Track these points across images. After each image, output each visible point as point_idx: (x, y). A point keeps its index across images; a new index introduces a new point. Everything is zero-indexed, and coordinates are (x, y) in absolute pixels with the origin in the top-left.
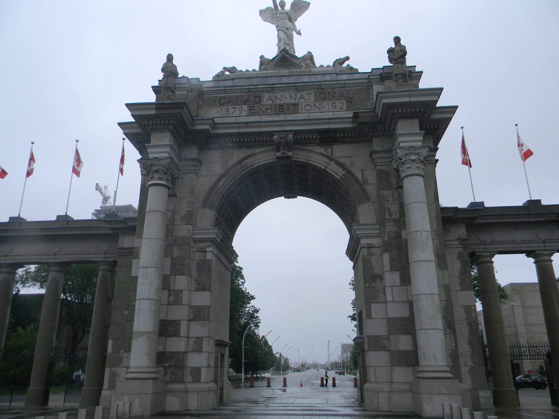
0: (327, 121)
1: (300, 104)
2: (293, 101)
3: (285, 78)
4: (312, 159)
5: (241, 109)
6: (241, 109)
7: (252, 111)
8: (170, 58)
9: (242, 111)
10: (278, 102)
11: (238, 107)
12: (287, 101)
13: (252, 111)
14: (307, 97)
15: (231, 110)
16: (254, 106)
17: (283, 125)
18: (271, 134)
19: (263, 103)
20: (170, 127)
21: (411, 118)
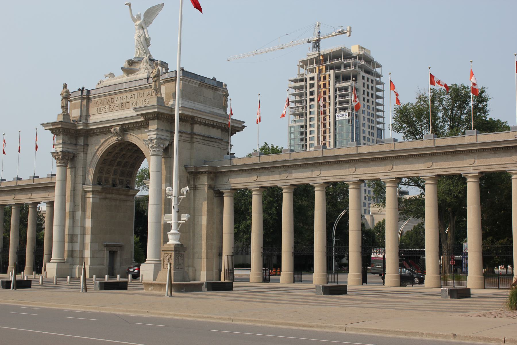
0: (132, 118)
1: (130, 102)
2: (128, 100)
3: (125, 84)
4: (132, 140)
5: (105, 108)
6: (105, 108)
7: (110, 109)
8: (65, 86)
9: (106, 109)
10: (122, 101)
11: (104, 106)
12: (125, 100)
13: (110, 109)
14: (133, 96)
15: (101, 110)
16: (111, 105)
17: (114, 122)
18: (111, 127)
19: (115, 103)
20: (62, 133)
21: (153, 119)
